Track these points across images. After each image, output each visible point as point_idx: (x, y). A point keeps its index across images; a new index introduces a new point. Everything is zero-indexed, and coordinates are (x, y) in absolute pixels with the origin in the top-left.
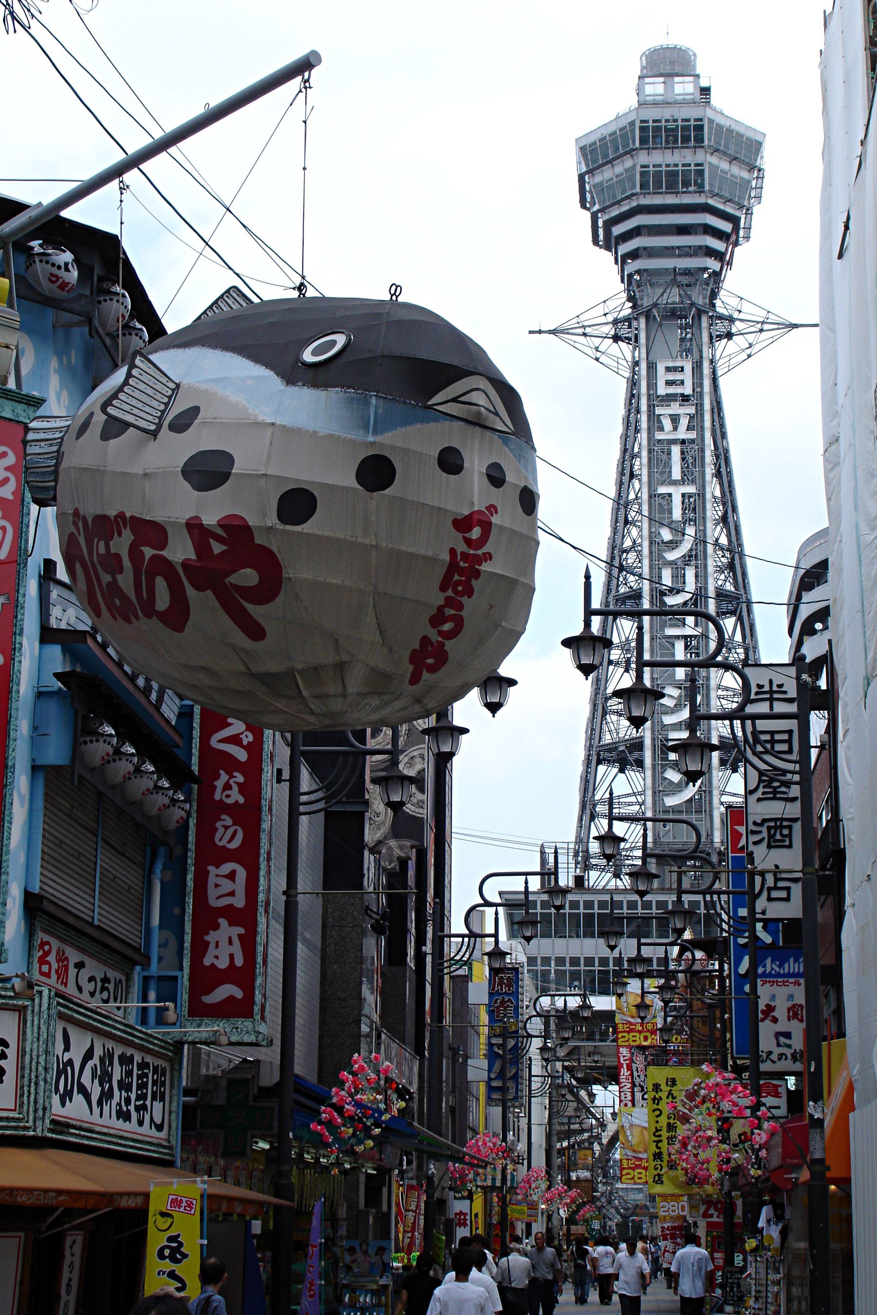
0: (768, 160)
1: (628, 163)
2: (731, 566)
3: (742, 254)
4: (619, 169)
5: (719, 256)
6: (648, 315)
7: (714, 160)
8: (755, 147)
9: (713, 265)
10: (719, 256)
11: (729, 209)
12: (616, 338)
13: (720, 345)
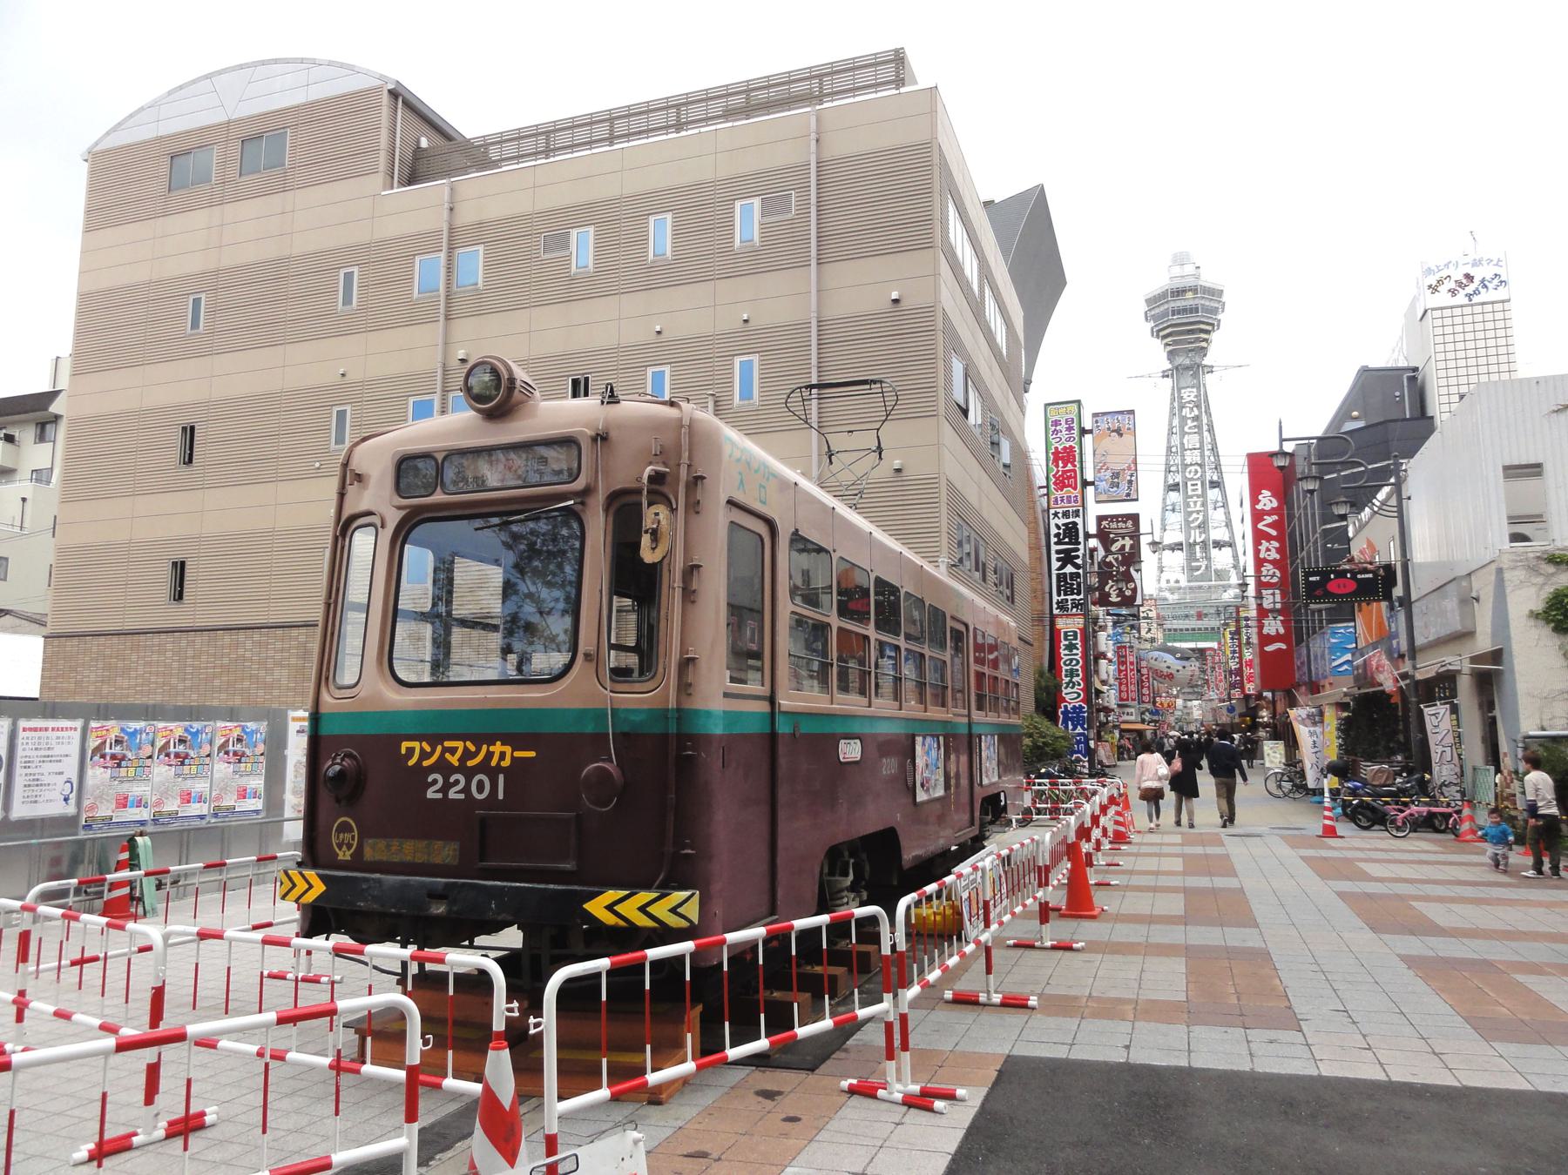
0: (1224, 299)
1: (1166, 306)
2: (1216, 468)
3: (1214, 336)
4: (1162, 309)
5: (1206, 340)
6: (1177, 368)
7: (1203, 302)
8: (1221, 292)
9: (1204, 344)
10: (1206, 340)
11: (1210, 321)
12: (1163, 377)
13: (1208, 376)
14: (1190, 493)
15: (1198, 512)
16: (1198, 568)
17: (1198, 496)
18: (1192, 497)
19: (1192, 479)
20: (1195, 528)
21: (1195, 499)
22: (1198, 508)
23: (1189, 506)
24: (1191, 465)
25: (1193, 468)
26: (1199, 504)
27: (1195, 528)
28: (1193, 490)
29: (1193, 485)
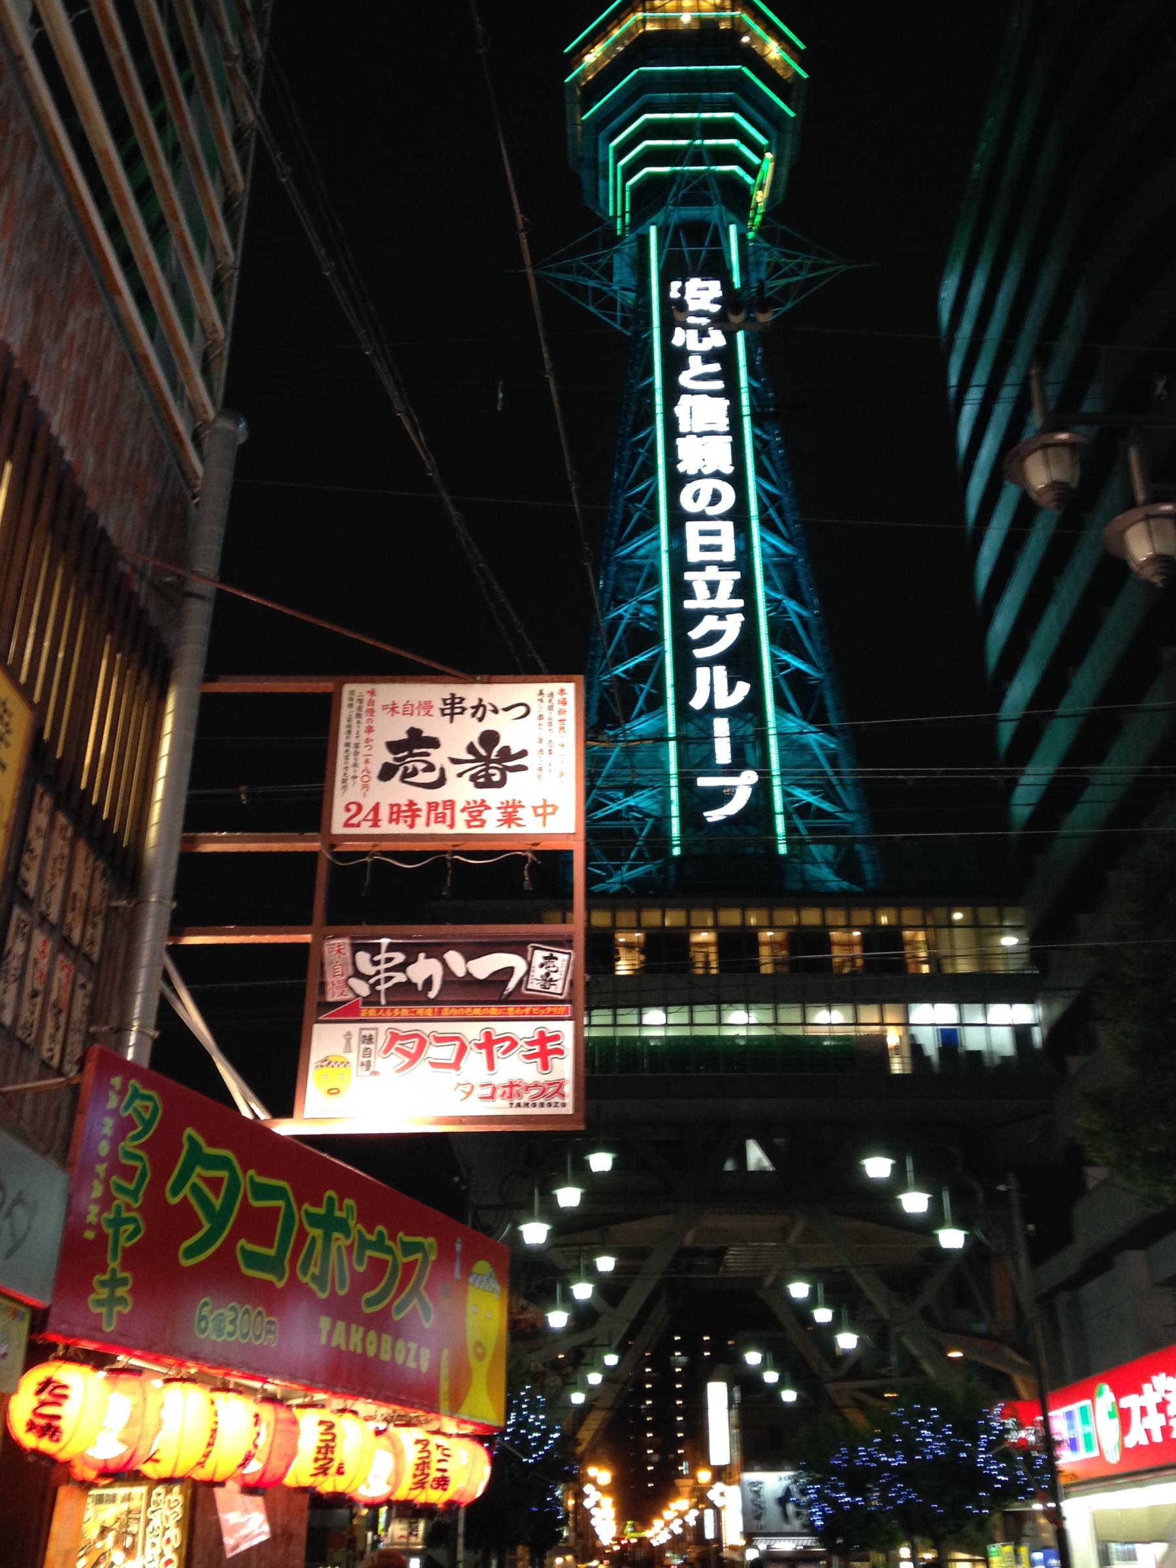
14: (694, 555)
15: (722, 614)
16: (721, 797)
17: (723, 566)
18: (700, 567)
19: (701, 517)
20: (710, 662)
21: (712, 573)
22: (723, 600)
23: (692, 596)
24: (700, 476)
25: (706, 487)
26: (726, 588)
27: (710, 662)
28: (705, 548)
29: (703, 533)
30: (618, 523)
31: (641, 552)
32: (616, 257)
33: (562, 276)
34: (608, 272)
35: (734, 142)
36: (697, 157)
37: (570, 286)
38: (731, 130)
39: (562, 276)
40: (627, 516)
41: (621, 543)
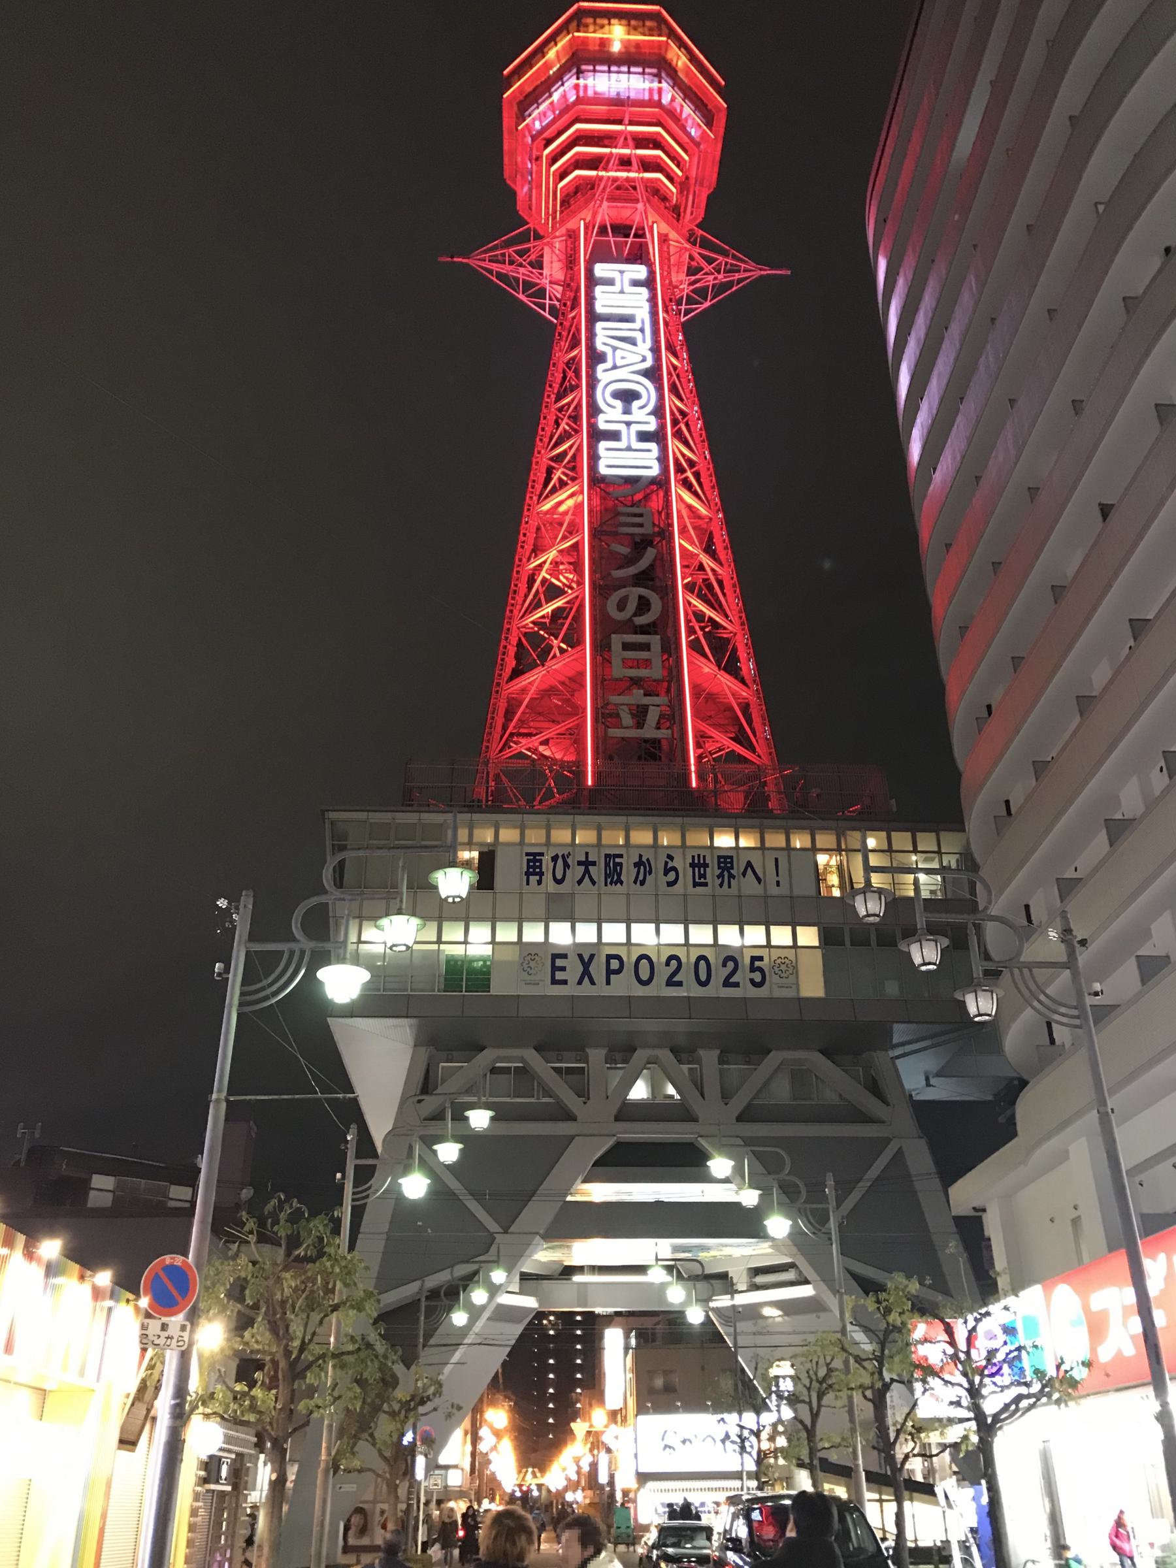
30: (542, 480)
31: (563, 508)
32: (547, 250)
33: (495, 267)
34: (538, 265)
35: (658, 129)
36: (625, 163)
37: (500, 276)
38: (656, 143)
39: (495, 267)
40: (550, 472)
41: (542, 498)
